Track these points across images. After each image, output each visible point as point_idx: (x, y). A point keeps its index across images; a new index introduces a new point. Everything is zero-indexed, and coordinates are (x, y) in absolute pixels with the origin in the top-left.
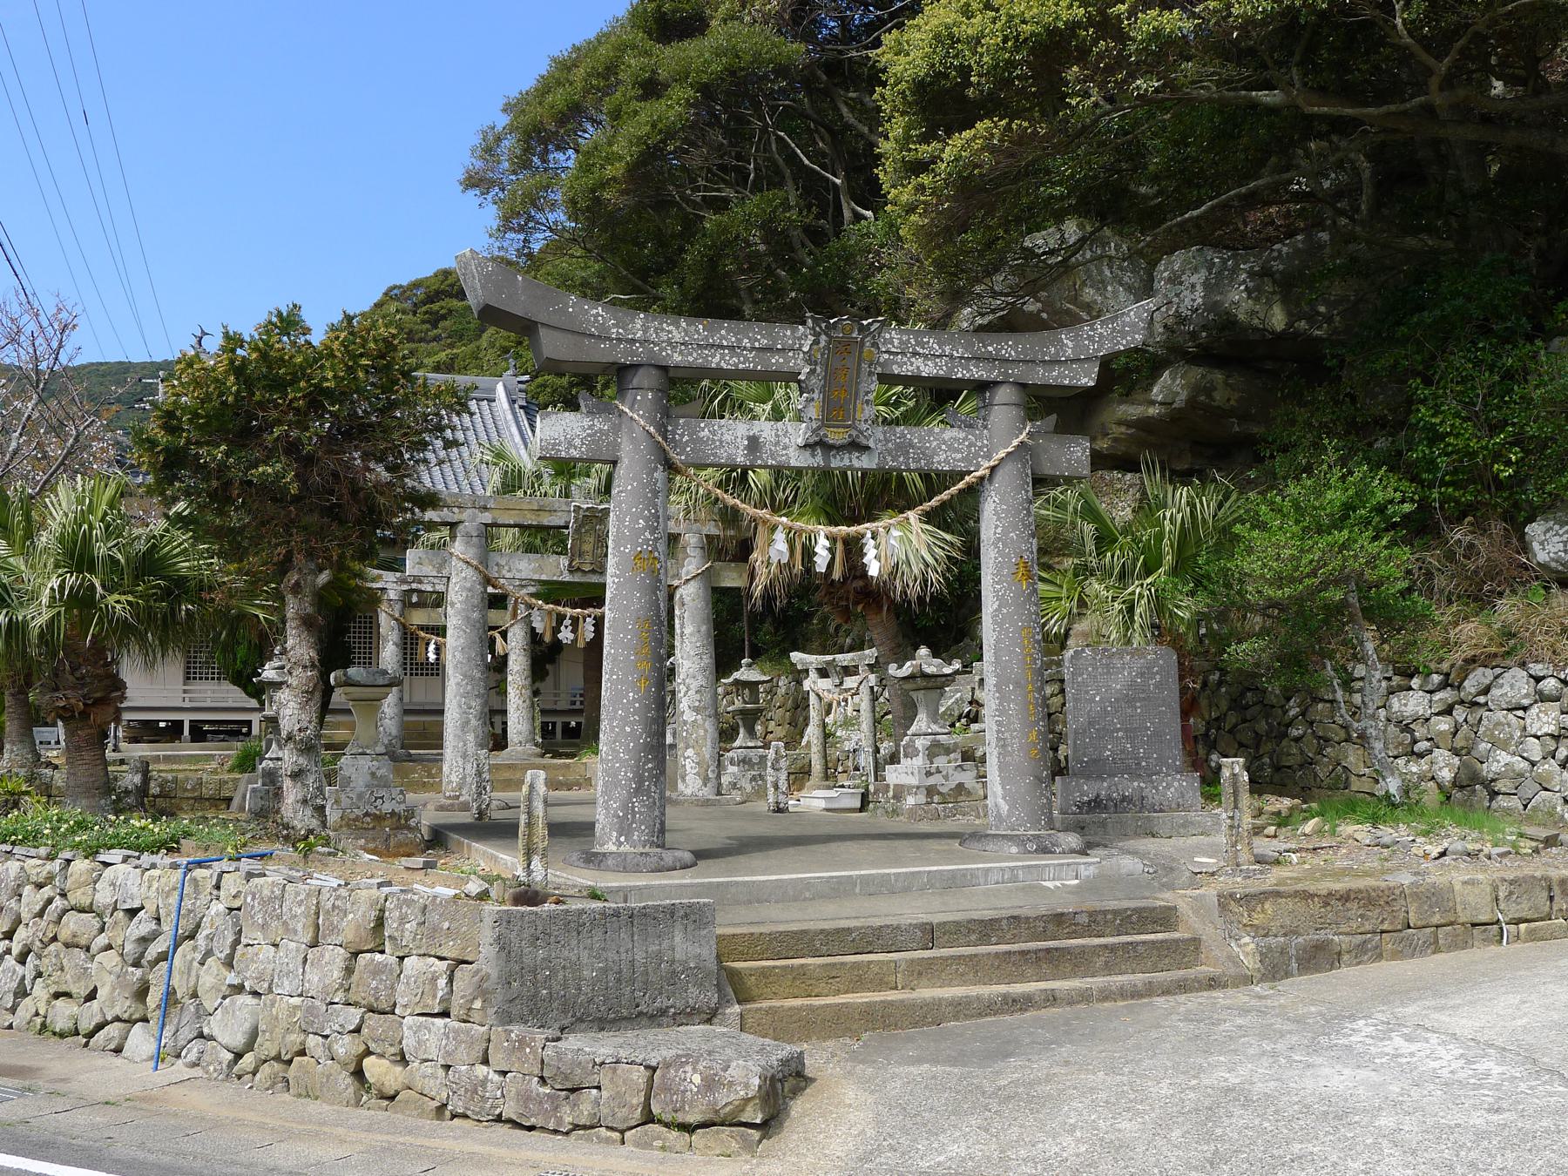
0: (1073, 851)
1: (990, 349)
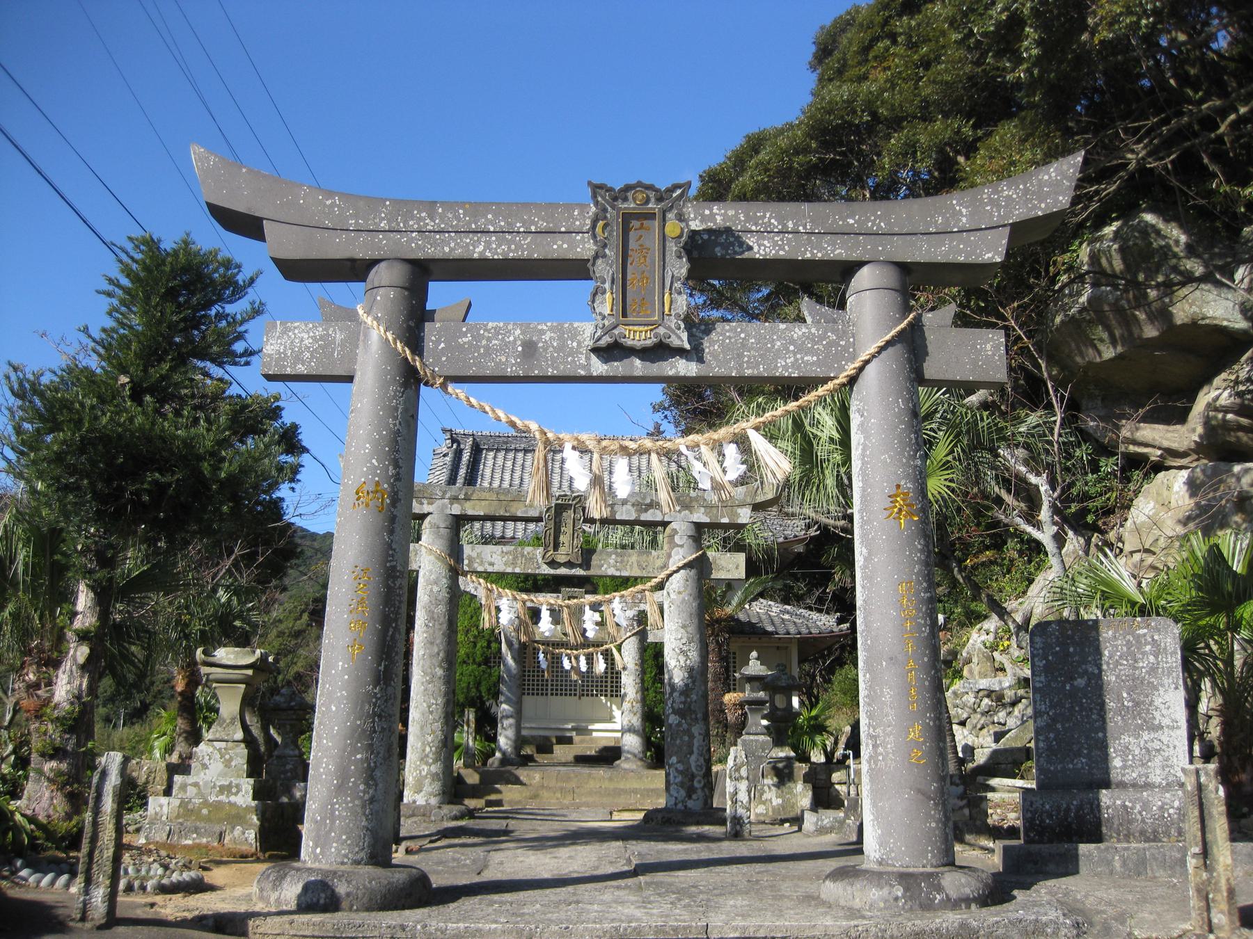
0: (967, 901)
1: (851, 221)
